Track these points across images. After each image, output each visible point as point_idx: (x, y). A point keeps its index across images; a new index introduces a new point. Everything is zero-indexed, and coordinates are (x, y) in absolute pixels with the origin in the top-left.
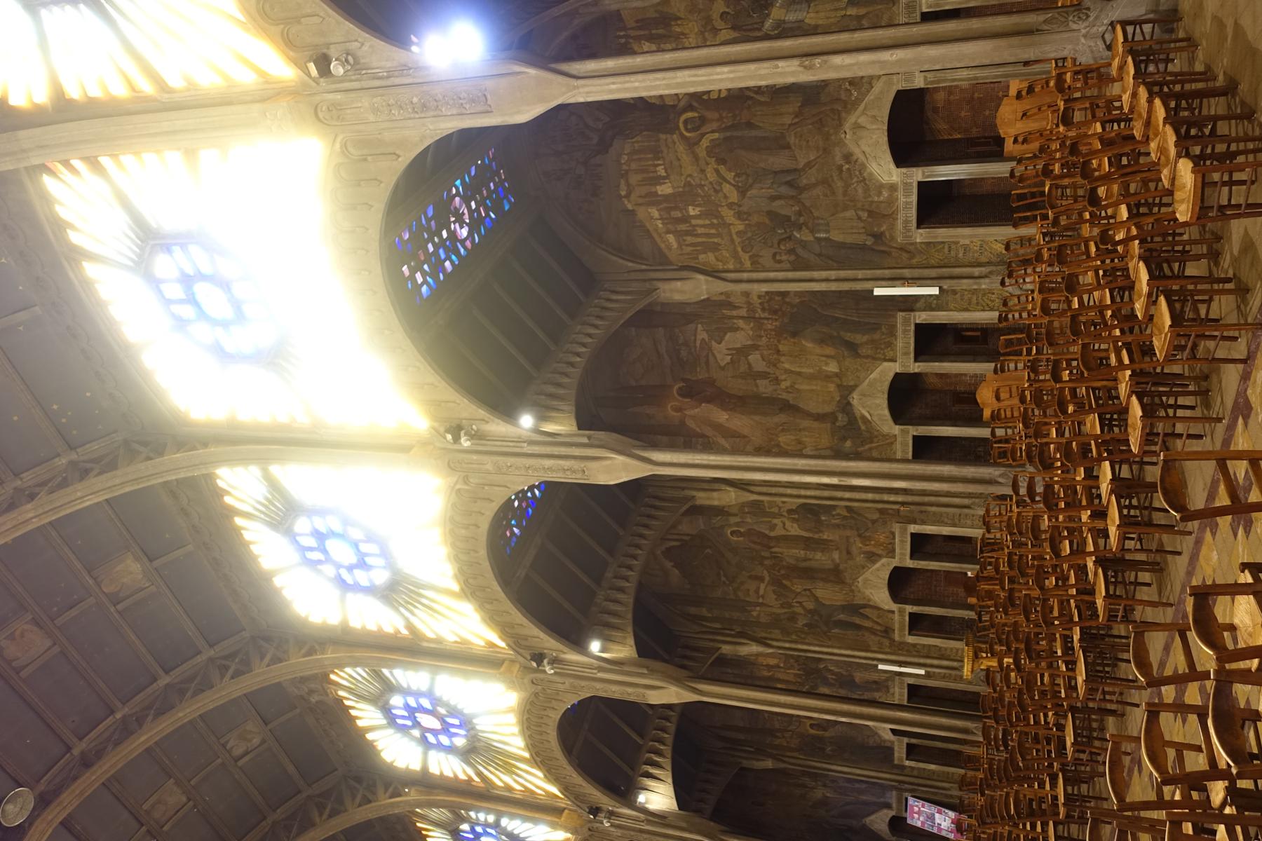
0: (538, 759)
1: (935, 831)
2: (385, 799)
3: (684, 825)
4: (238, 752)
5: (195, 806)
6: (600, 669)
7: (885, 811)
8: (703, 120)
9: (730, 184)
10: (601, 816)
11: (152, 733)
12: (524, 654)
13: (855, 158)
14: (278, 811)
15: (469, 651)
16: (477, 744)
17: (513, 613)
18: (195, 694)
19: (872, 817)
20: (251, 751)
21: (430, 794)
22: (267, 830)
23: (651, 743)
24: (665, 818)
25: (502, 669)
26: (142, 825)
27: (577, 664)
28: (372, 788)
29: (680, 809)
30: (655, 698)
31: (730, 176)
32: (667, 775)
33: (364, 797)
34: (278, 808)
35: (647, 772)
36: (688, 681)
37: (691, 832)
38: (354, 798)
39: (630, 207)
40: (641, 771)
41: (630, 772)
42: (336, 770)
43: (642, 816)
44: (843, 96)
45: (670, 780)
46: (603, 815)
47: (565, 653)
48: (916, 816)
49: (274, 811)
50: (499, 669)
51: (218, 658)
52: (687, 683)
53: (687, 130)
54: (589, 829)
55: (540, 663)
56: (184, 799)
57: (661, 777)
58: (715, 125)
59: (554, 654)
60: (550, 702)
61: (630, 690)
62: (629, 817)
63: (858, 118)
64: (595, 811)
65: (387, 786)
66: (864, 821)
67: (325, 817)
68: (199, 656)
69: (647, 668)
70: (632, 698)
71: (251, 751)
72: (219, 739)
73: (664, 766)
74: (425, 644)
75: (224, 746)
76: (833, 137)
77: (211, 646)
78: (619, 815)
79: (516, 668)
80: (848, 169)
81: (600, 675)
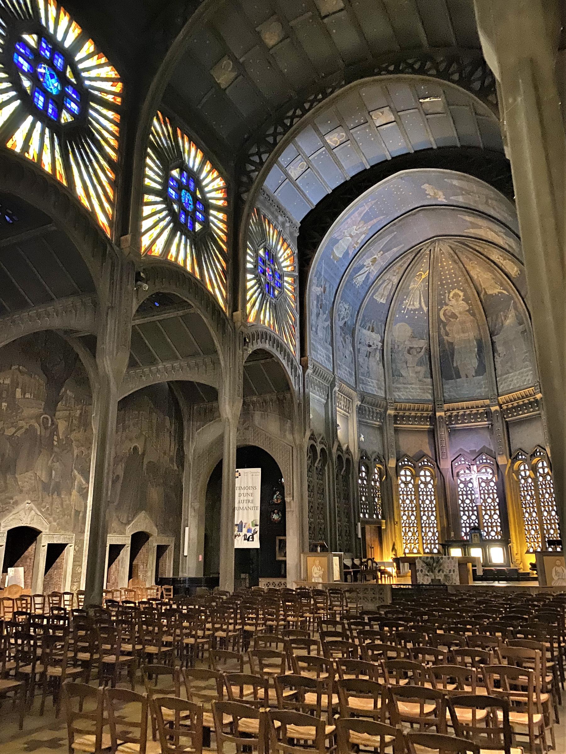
8: (46, 428)
9: (15, 433)
13: (15, 507)
31: (18, 434)
39: (13, 368)
44: (44, 504)
53: (44, 417)
58: (43, 434)
63: (35, 511)
76: (27, 496)
80: (10, 503)
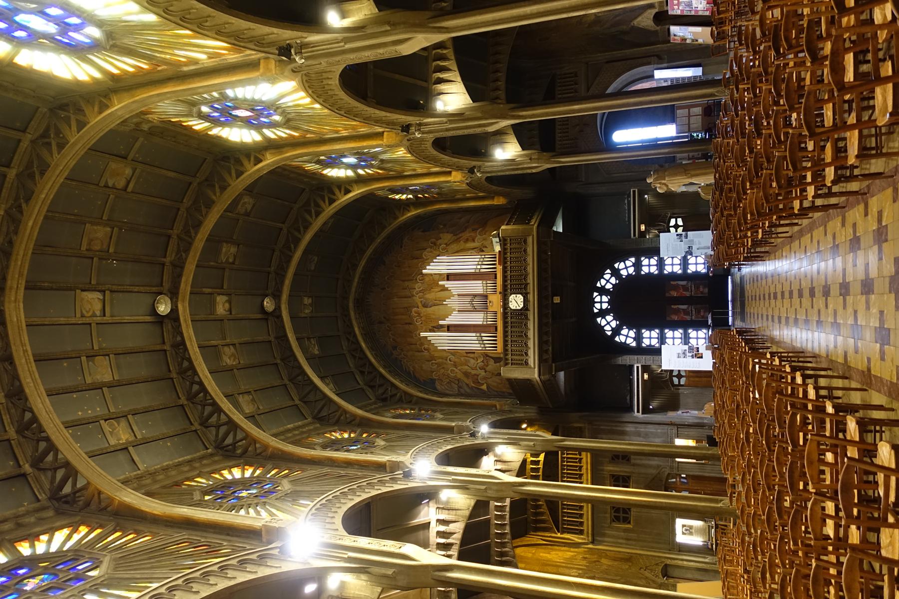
0: (342, 113)
1: (693, 13)
2: (252, 168)
3: (479, 115)
4: (121, 184)
5: (121, 229)
6: (346, 40)
7: (649, 11)
10: (413, 129)
11: (34, 216)
12: (271, 51)
14: (184, 201)
15: (225, 62)
16: (290, 116)
17: (234, 21)
18: (42, 173)
19: (640, 19)
20: (131, 178)
21: (281, 153)
22: (185, 215)
23: (434, 52)
24: (463, 114)
25: (261, 70)
26: (93, 258)
27: (323, 43)
28: (239, 162)
29: (473, 102)
30: (407, 49)
32: (455, 75)
33: (236, 170)
34: (183, 198)
35: (439, 78)
36: (431, 23)
37: (486, 119)
38: (230, 174)
40: (433, 80)
41: (424, 84)
42: (206, 159)
43: (444, 119)
45: (459, 79)
46: (413, 128)
47: (306, 38)
48: (676, 7)
49: (182, 202)
50: (258, 69)
51: (37, 139)
52: (431, 25)
54: (408, 140)
55: (288, 56)
56: (109, 229)
57: (449, 79)
59: (298, 41)
60: (322, 76)
61: (381, 51)
62: (434, 123)
64: (406, 128)
65: (248, 156)
66: (632, 24)
67: (218, 194)
68: (21, 144)
69: (389, 23)
70: (386, 56)
71: (131, 178)
72: (98, 185)
73: (451, 68)
74: (185, 69)
75: (106, 186)
77: (24, 131)
78: (426, 124)
79: (272, 64)
81: (348, 46)
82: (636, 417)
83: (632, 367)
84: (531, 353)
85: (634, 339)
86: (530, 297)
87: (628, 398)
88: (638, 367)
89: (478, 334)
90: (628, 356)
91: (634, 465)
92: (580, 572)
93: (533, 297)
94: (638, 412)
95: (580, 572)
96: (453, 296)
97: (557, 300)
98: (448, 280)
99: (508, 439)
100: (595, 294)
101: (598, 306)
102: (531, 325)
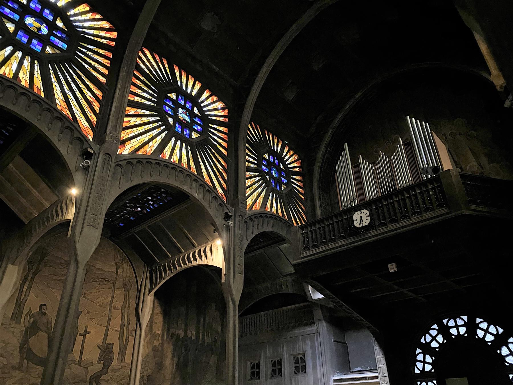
82: (329, 380)
83: (375, 370)
84: (316, 251)
85: (423, 371)
86: (373, 233)
87: (359, 369)
88: (377, 378)
89: (355, 197)
90: (385, 365)
91: (291, 379)
92: (193, 338)
93: (372, 236)
94: (335, 381)
95: (193, 338)
96: (390, 158)
97: (392, 268)
98: (405, 145)
99: (229, 249)
100: (465, 318)
101: (452, 323)
102: (342, 242)
